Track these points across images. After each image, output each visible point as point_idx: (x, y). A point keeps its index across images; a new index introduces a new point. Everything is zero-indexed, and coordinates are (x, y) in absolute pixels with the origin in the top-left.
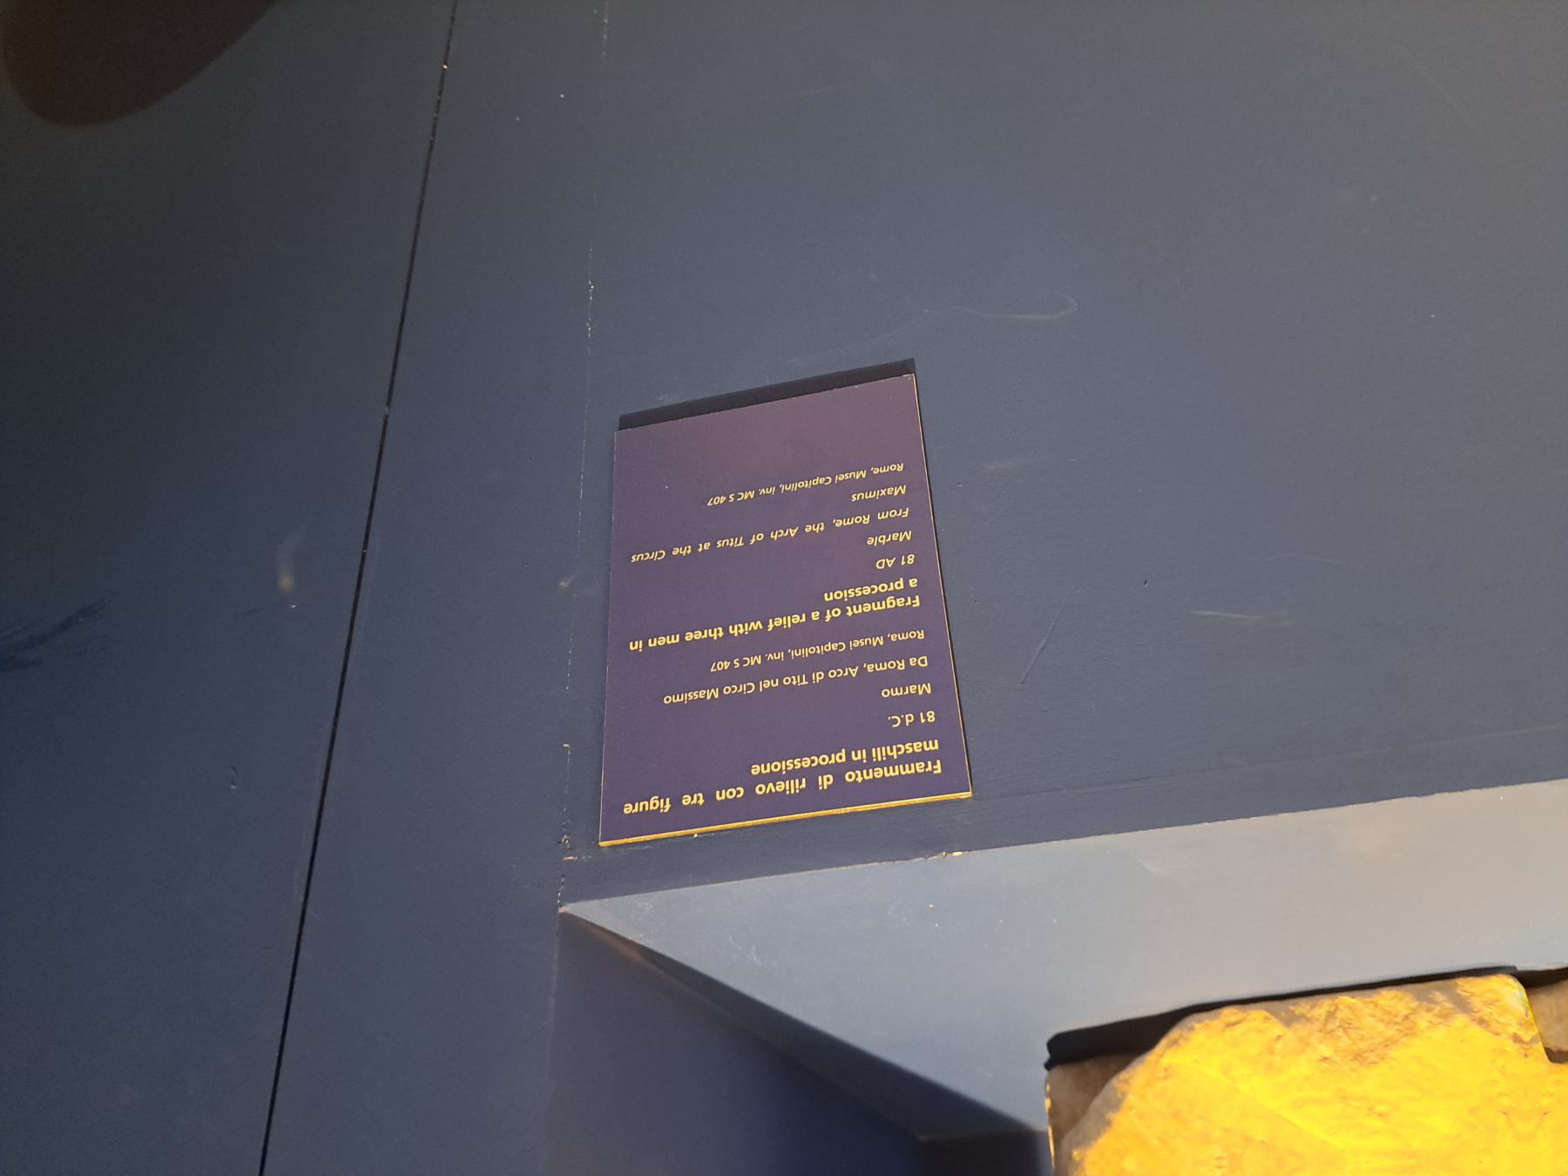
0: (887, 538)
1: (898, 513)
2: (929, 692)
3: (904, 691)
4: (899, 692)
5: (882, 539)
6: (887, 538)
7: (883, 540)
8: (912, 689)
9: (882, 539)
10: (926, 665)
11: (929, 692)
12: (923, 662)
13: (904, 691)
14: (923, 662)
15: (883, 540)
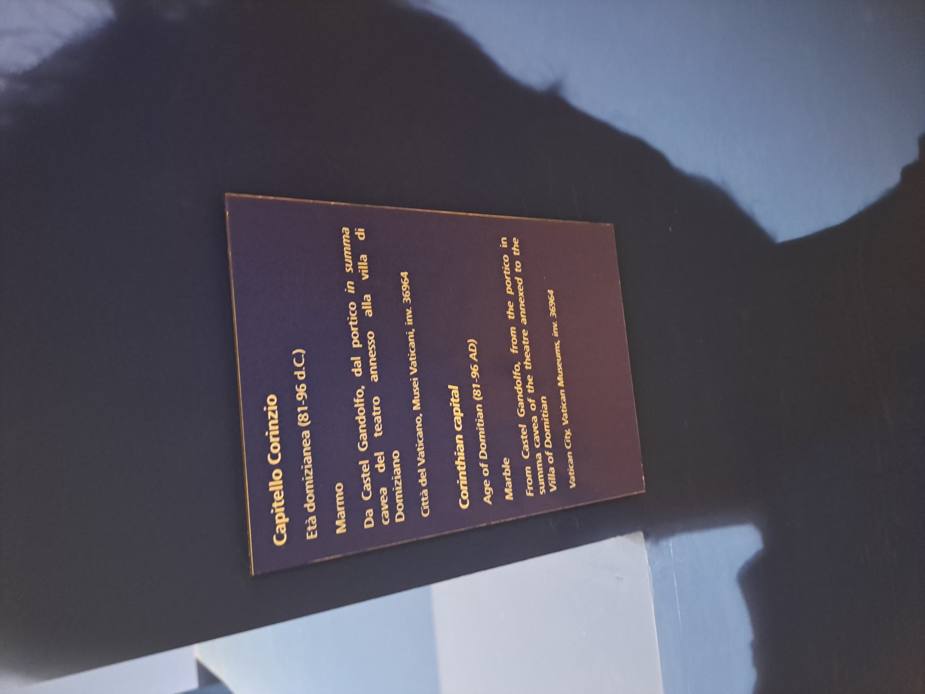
0: (508, 477)
1: (530, 486)
2: (338, 531)
3: (340, 506)
4: (340, 501)
5: (508, 472)
6: (508, 477)
7: (507, 473)
8: (341, 512)
9: (508, 472)
10: (366, 526)
11: (338, 531)
12: (369, 523)
13: (340, 506)
14: (369, 523)
15: (507, 473)
